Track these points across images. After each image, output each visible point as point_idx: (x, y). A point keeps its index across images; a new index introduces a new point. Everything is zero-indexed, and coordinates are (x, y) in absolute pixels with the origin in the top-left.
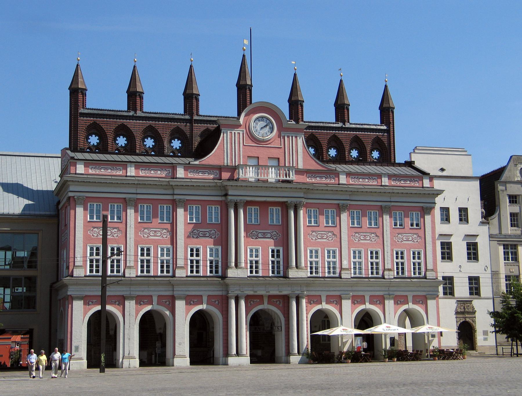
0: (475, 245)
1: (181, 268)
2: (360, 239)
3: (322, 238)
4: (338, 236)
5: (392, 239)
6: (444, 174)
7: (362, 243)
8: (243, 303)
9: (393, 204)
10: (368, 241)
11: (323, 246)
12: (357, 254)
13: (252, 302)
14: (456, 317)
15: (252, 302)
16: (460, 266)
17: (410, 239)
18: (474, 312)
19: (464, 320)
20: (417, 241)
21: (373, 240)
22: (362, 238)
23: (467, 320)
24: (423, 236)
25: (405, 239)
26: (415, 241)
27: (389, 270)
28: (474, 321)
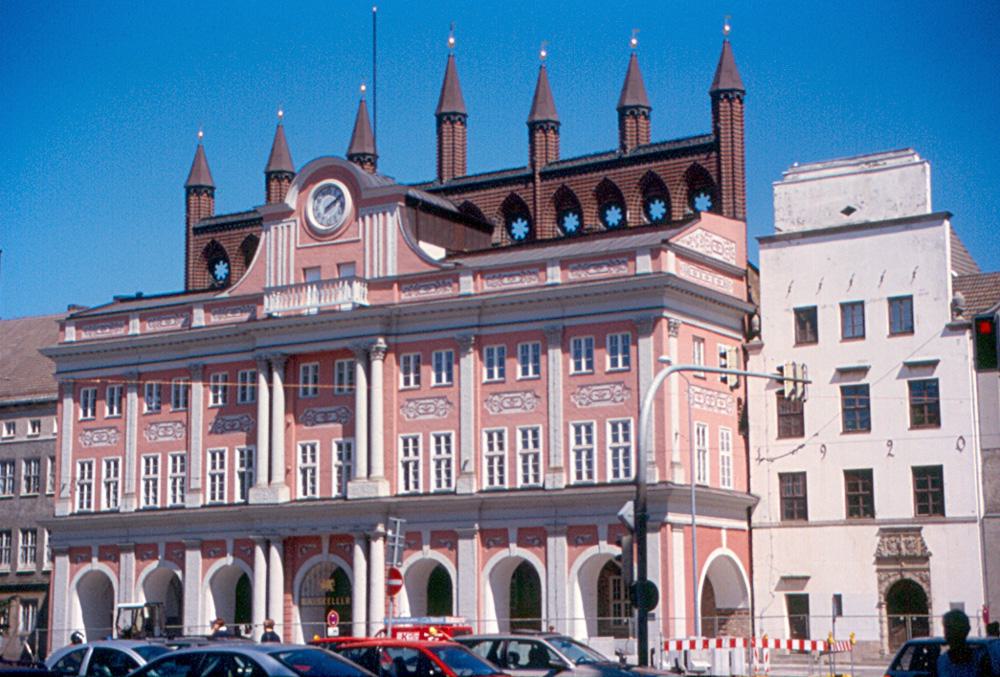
0: (864, 390)
1: (197, 490)
2: (502, 407)
3: (427, 412)
4: (456, 405)
5: (567, 400)
6: (855, 218)
7: (506, 416)
8: (275, 553)
9: (567, 322)
10: (519, 411)
11: (427, 427)
12: (497, 438)
13: (304, 550)
14: (878, 571)
15: (304, 550)
16: (890, 443)
17: (608, 396)
18: (926, 558)
19: (898, 577)
20: (622, 400)
21: (528, 406)
22: (506, 405)
23: (908, 576)
24: (635, 387)
25: (595, 398)
26: (619, 399)
27: (557, 470)
28: (928, 581)
